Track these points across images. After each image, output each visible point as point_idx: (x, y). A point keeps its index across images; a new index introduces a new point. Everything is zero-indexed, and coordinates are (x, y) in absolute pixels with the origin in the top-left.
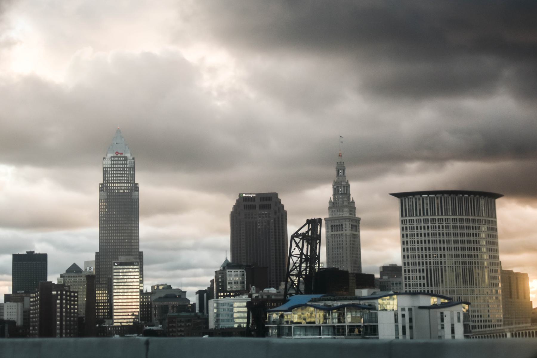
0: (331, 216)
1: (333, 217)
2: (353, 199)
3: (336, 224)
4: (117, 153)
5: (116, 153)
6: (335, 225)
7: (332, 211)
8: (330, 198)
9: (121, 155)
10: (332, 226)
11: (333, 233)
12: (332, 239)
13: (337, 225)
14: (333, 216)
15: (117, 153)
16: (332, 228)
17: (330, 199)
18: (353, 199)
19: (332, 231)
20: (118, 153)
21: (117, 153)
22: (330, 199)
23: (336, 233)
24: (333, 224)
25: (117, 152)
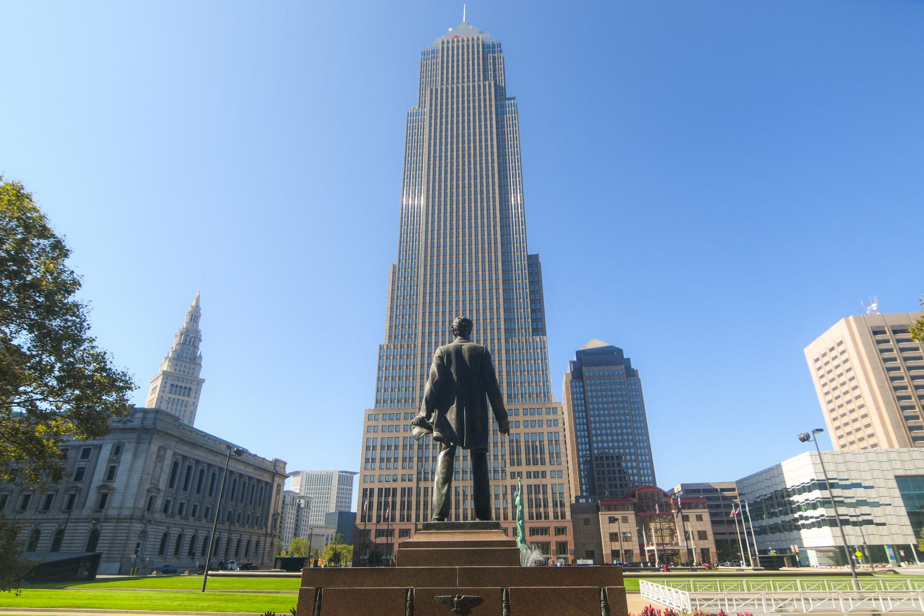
1: (175, 373)
3: (180, 384)
6: (177, 386)
7: (177, 365)
12: (168, 404)
13: (181, 387)
16: (171, 390)
19: (171, 393)
23: (176, 397)
24: (175, 383)
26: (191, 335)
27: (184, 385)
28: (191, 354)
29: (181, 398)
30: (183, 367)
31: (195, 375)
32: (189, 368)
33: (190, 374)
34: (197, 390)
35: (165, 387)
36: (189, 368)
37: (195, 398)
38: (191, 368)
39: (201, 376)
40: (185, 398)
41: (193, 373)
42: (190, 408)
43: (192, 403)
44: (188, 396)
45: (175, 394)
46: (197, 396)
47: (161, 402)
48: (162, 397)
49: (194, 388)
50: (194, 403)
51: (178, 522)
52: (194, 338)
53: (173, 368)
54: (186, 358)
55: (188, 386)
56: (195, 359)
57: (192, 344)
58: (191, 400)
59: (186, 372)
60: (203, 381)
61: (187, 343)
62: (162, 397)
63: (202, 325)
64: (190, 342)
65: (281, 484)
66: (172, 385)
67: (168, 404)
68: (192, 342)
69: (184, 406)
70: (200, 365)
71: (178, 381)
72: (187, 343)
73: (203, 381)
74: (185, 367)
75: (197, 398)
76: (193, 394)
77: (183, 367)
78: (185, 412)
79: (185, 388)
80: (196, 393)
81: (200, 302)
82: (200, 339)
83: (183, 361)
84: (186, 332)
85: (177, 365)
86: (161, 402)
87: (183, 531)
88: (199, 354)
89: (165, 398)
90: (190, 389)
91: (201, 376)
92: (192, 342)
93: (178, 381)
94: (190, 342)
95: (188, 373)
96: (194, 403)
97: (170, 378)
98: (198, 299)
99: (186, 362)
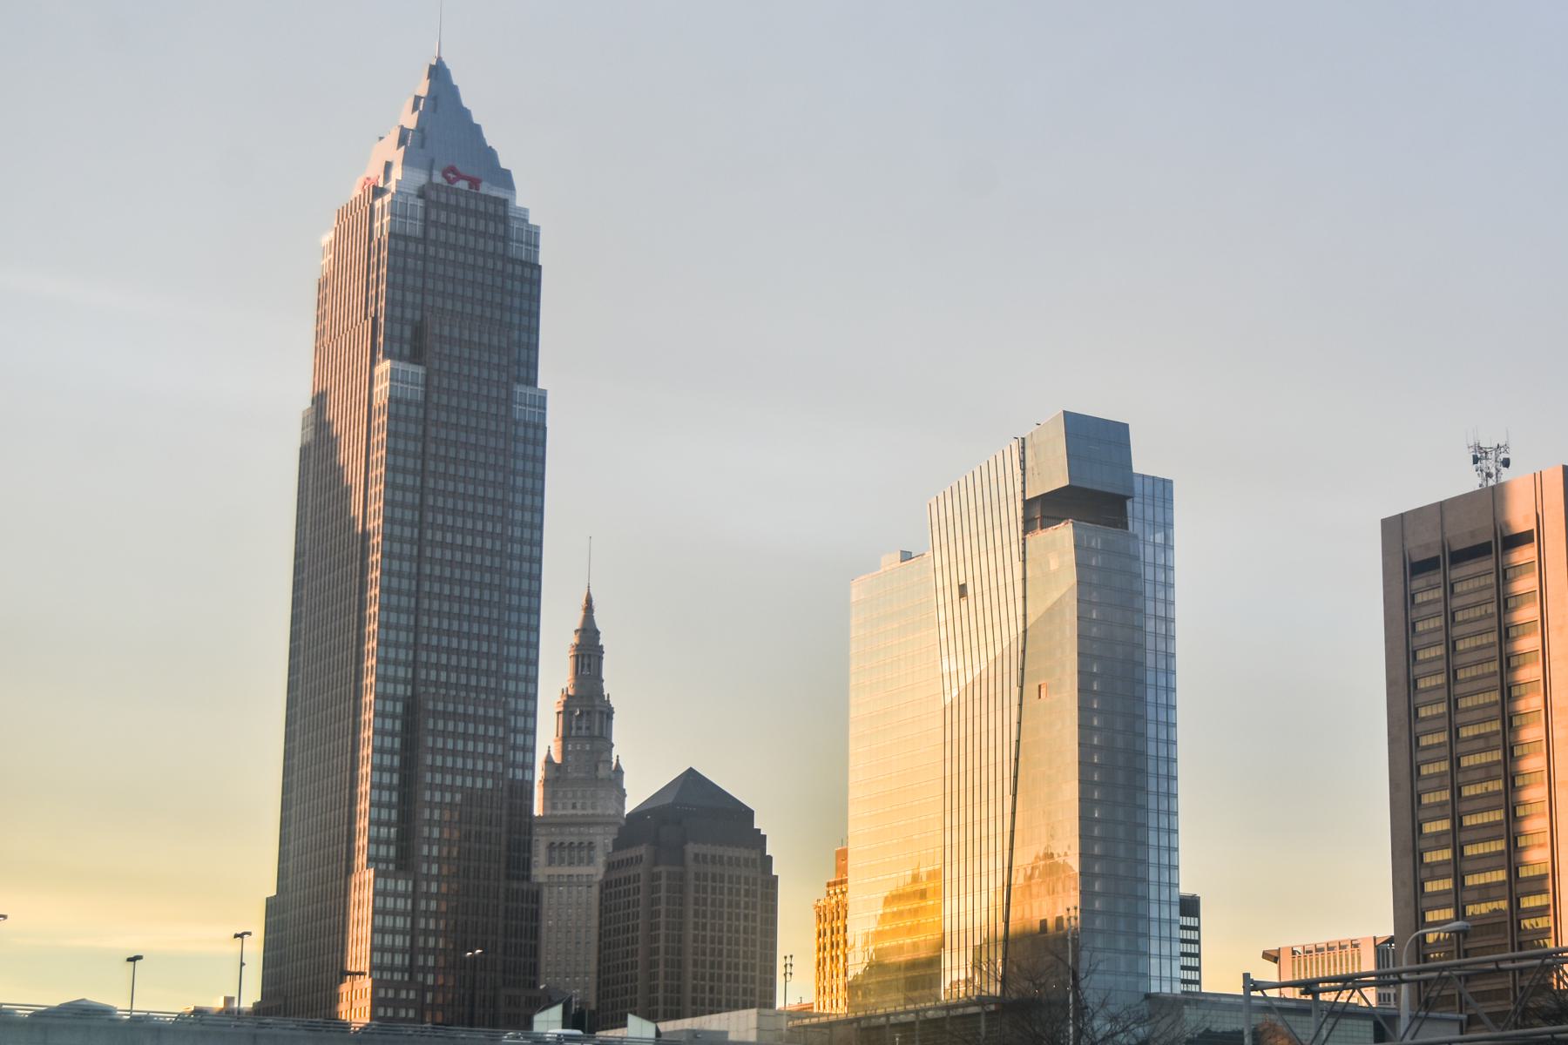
0: (549, 812)
2: (618, 760)
3: (567, 840)
4: (451, 176)
5: (444, 175)
8: (549, 747)
9: (470, 187)
10: (551, 846)
14: (555, 812)
15: (451, 172)
17: (549, 751)
18: (618, 760)
20: (460, 177)
21: (451, 172)
22: (549, 751)
23: (565, 870)
24: (557, 840)
25: (452, 169)
29: (575, 870)
30: (570, 795)
41: (593, 807)
44: (591, 861)
52: (589, 713)
53: (548, 804)
55: (586, 840)
57: (583, 732)
59: (579, 806)
61: (573, 732)
77: (570, 795)
81: (595, 615)
94: (579, 728)
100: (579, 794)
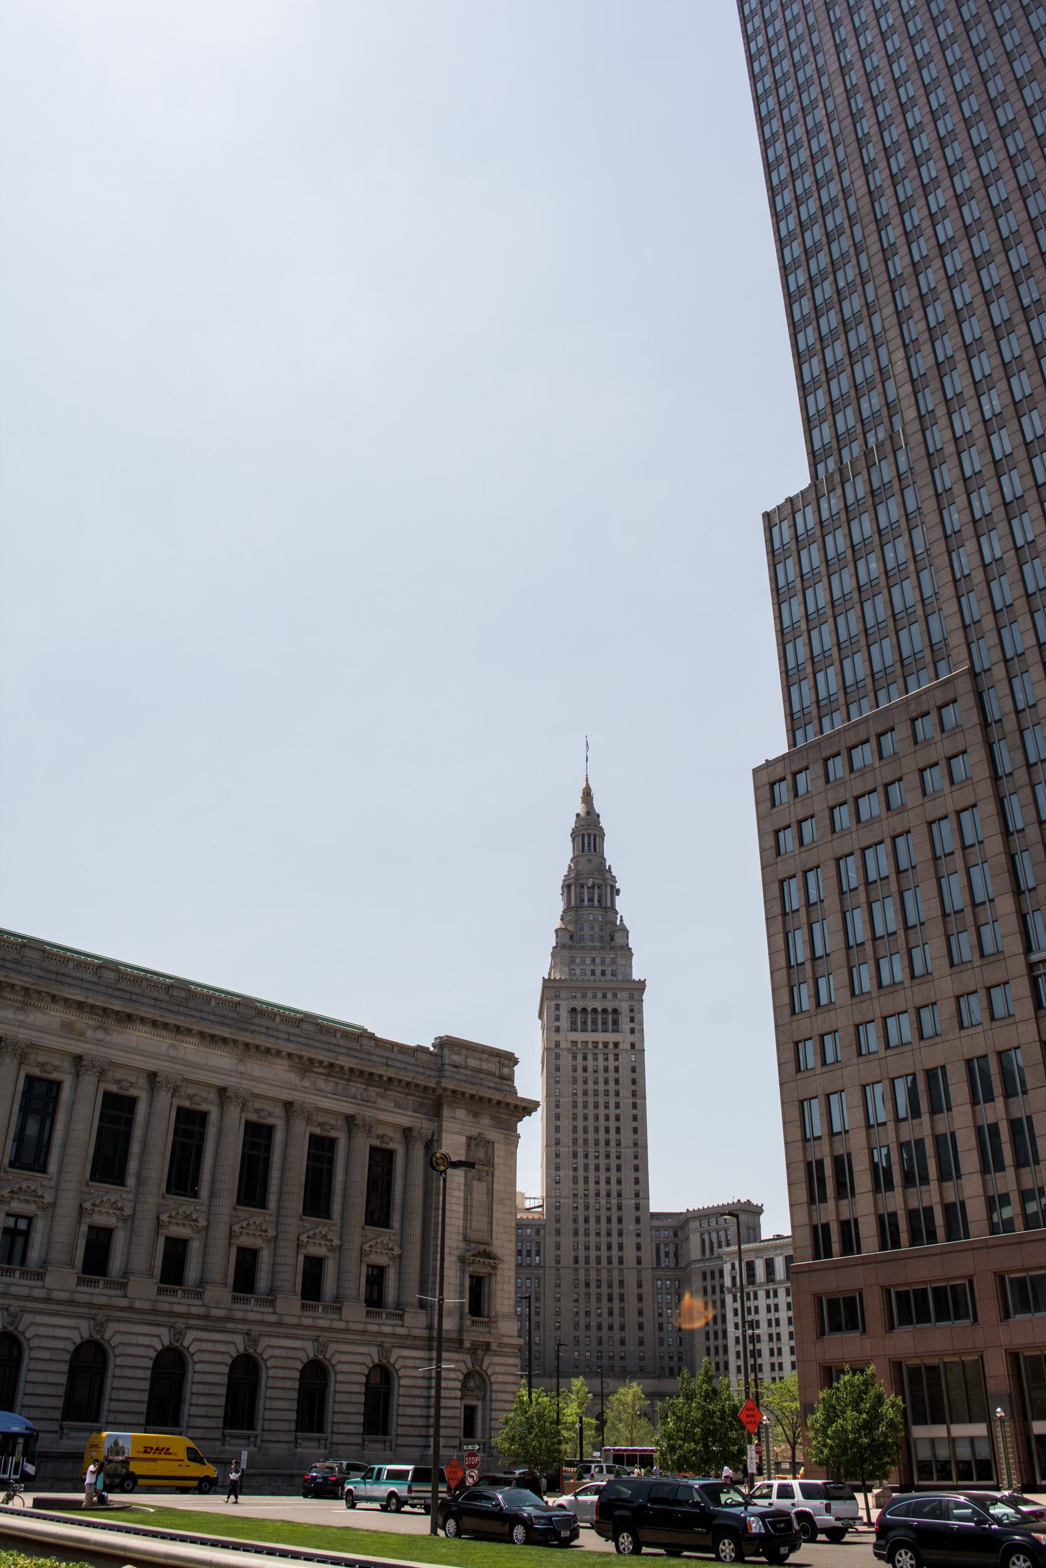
3: (590, 1005)
6: (584, 1010)
7: (572, 961)
11: (579, 1036)
12: (574, 1058)
13: (595, 1010)
16: (573, 1023)
19: (574, 1030)
23: (590, 1037)
24: (579, 1004)
26: (590, 884)
27: (599, 1005)
28: (602, 930)
29: (600, 1037)
30: (588, 962)
31: (620, 977)
32: (603, 963)
33: (609, 977)
34: (632, 1010)
35: (557, 1019)
36: (603, 963)
37: (632, 1031)
38: (608, 961)
39: (636, 976)
40: (611, 1037)
42: (625, 1061)
43: (628, 1047)
44: (616, 1030)
45: (584, 1030)
46: (637, 1027)
47: (557, 1057)
48: (557, 1045)
49: (624, 1007)
50: (633, 1046)
51: (354, 1326)
53: (566, 969)
54: (592, 938)
55: (610, 1006)
56: (612, 939)
58: (624, 1038)
59: (598, 972)
60: (641, 986)
61: (586, 902)
62: (557, 1045)
63: (613, 853)
64: (591, 900)
65: (492, 1134)
66: (574, 1010)
67: (574, 1058)
68: (596, 898)
69: (611, 1057)
70: (627, 952)
71: (584, 996)
72: (586, 902)
73: (641, 986)
74: (593, 960)
75: (637, 1029)
76: (625, 1025)
78: (617, 1070)
79: (605, 1011)
80: (632, 1020)
82: (612, 887)
83: (583, 948)
84: (576, 879)
85: (572, 961)
86: (557, 1057)
87: (323, 1348)
88: (618, 922)
89: (563, 1045)
90: (615, 1011)
91: (636, 976)
92: (596, 898)
93: (584, 996)
95: (603, 973)
96: (633, 1046)
97: (563, 994)
98: (587, 796)
99: (594, 948)
100: (598, 961)
